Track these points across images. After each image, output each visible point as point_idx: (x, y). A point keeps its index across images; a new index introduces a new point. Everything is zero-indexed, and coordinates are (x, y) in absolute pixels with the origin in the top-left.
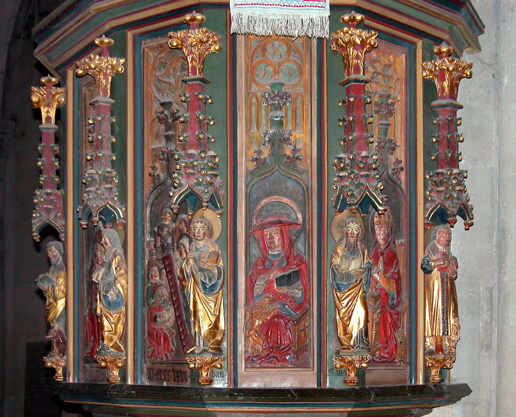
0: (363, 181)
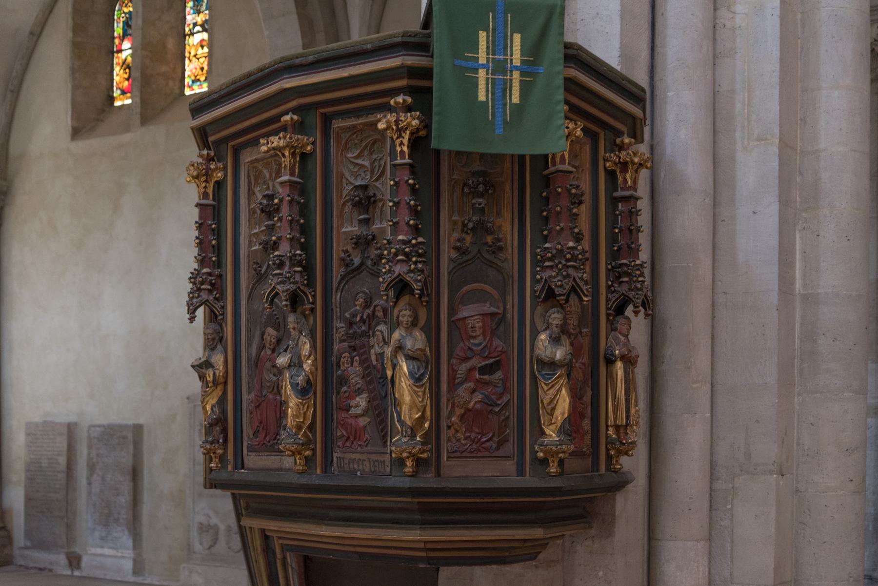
0: (571, 271)
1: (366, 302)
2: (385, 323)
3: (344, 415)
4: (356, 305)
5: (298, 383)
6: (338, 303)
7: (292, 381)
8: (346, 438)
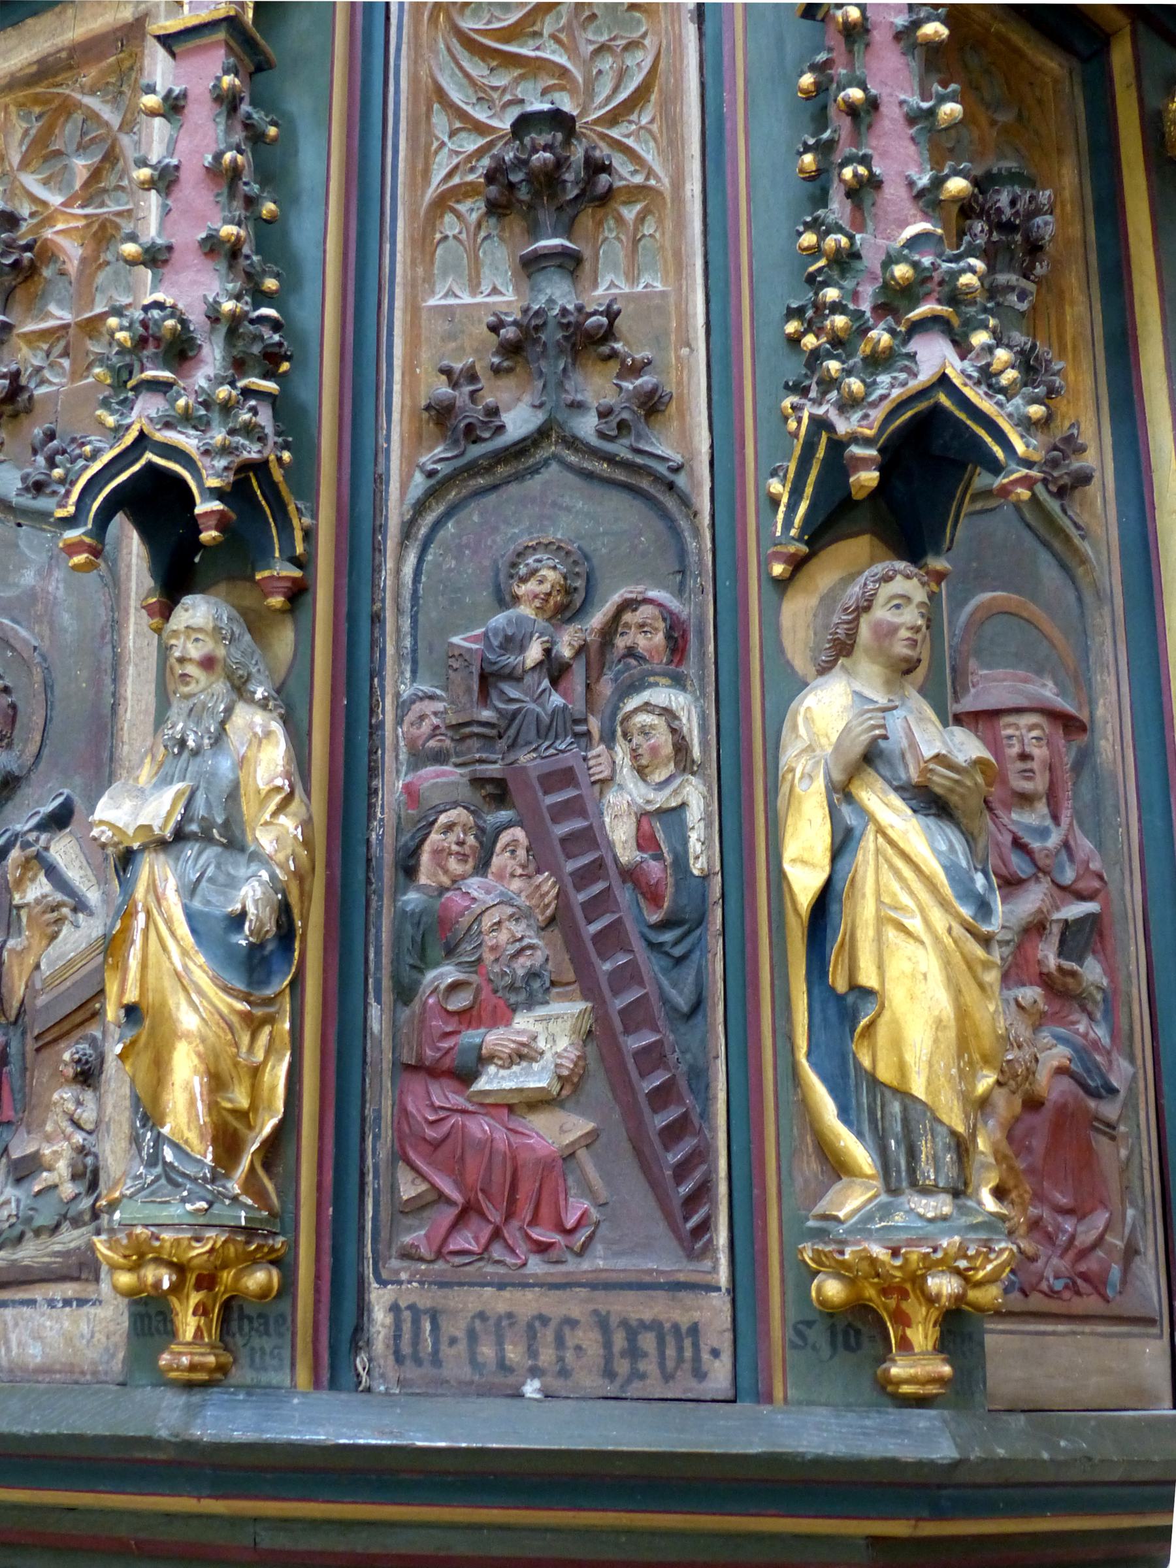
1: (569, 591)
2: (678, 681)
3: (444, 1095)
4: (516, 599)
5: (239, 918)
6: (407, 594)
7: (197, 904)
8: (451, 1213)
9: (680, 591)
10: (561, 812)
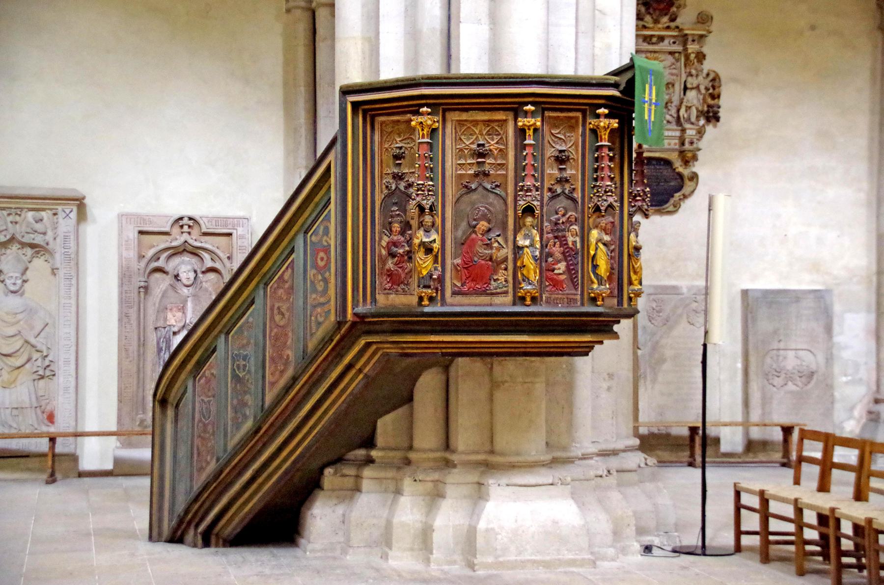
9: (576, 213)
10: (564, 240)
